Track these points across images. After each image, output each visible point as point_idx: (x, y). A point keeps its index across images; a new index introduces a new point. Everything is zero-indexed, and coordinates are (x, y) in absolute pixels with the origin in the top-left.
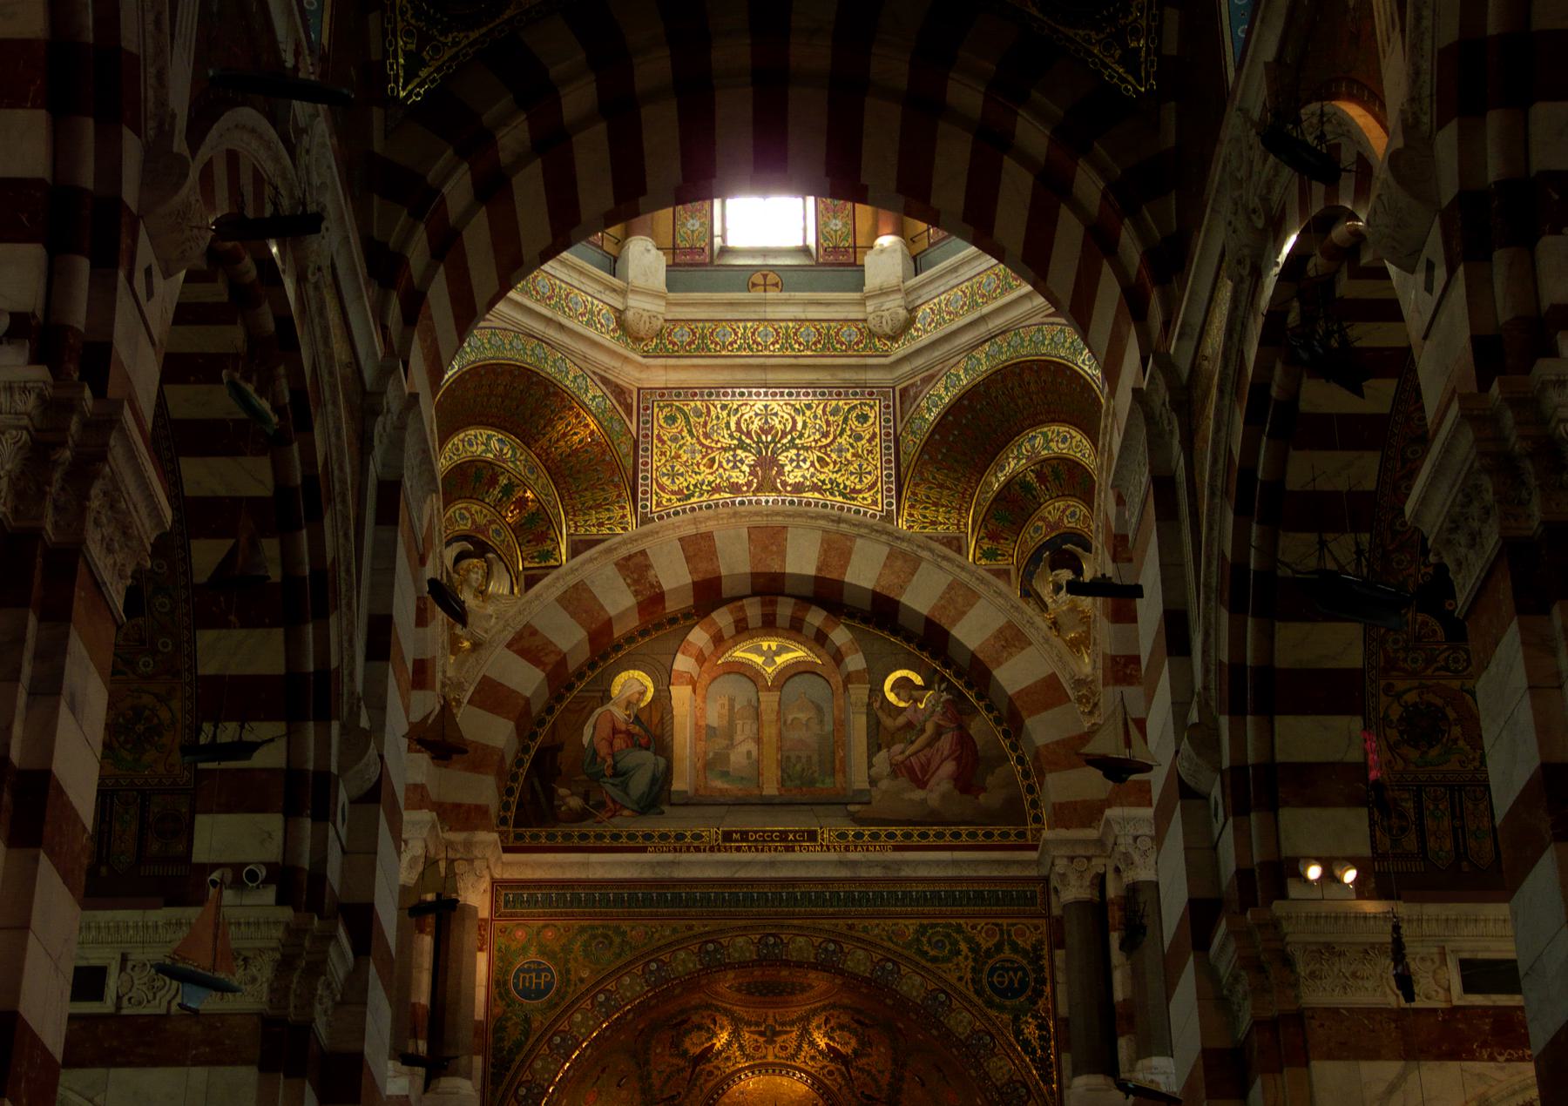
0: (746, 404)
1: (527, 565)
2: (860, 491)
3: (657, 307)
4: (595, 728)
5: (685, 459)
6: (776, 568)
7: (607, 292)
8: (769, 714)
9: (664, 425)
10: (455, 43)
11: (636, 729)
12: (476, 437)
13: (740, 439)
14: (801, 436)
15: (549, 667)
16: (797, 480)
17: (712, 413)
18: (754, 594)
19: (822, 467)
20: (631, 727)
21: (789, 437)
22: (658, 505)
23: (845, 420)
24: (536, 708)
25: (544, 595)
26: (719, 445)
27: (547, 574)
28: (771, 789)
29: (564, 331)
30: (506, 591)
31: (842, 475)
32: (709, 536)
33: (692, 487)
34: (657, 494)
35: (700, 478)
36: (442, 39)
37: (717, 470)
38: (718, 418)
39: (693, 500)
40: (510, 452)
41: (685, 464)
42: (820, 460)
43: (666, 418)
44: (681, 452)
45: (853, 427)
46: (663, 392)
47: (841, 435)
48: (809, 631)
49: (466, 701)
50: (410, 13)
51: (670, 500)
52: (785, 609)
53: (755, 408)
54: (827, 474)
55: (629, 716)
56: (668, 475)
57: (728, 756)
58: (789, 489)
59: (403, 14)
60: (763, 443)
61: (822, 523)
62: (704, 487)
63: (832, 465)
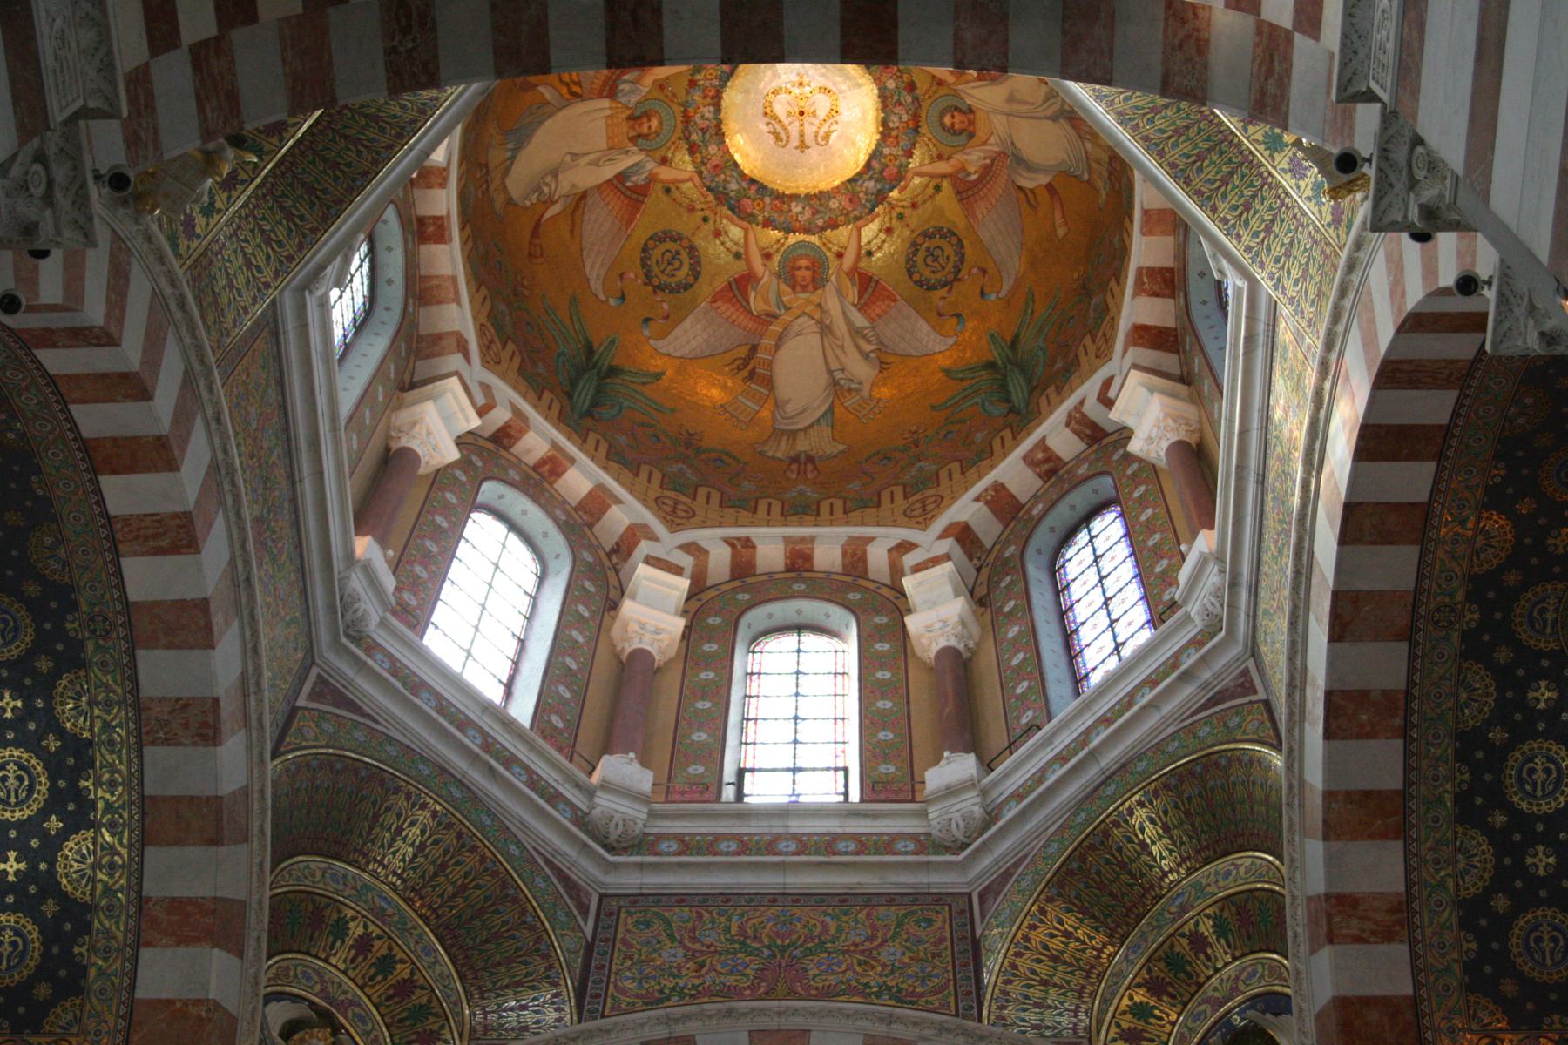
2: (922, 995)
7: (567, 785)
23: (900, 924)
26: (713, 949)
29: (494, 776)
33: (667, 991)
34: (613, 998)
35: (681, 982)
37: (707, 973)
38: (713, 923)
44: (655, 955)
46: (636, 899)
47: (893, 939)
54: (873, 978)
60: (777, 947)
61: (861, 1023)
63: (879, 969)
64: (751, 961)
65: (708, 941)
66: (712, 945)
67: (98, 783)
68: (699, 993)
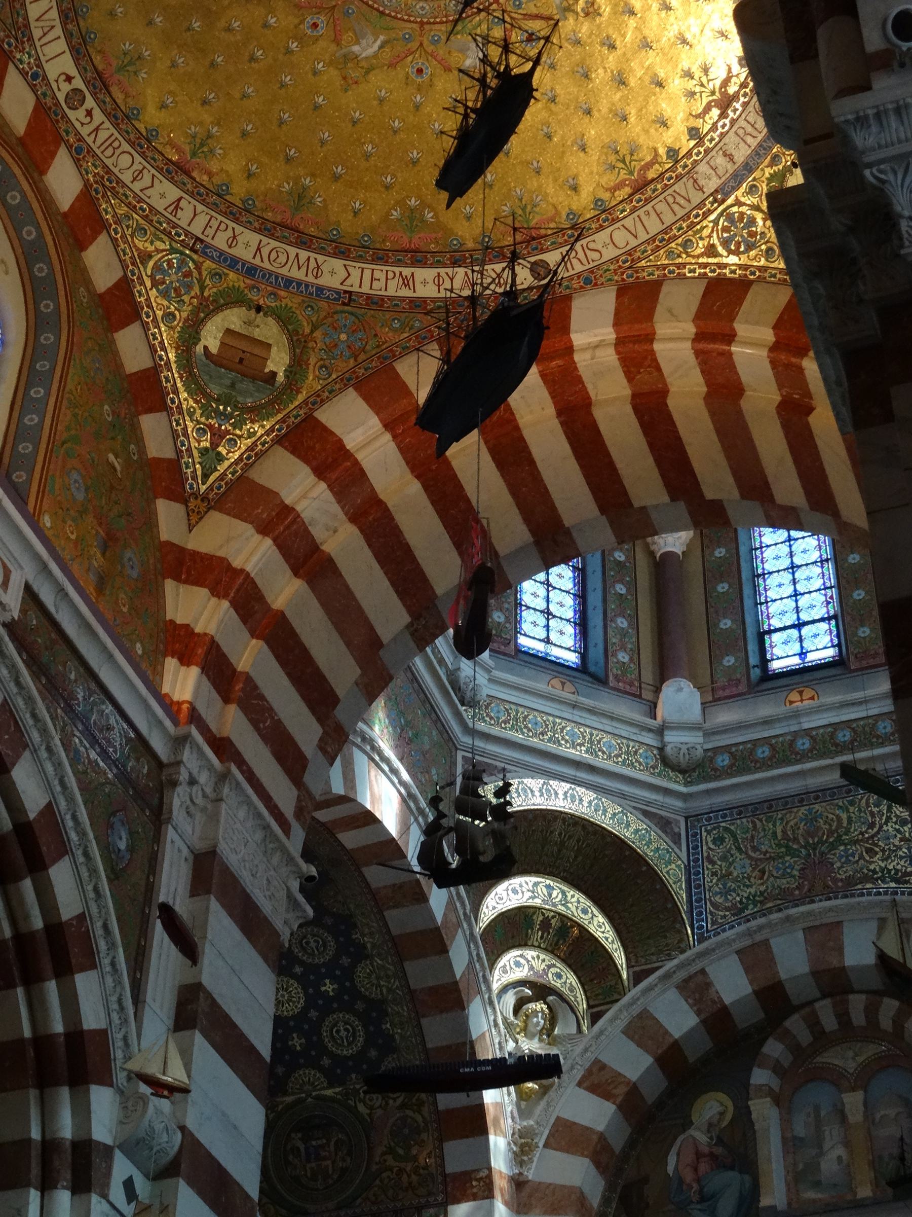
0: (791, 812)
1: (592, 1003)
3: (694, 739)
4: (678, 1155)
5: (735, 874)
6: (835, 963)
8: (855, 1115)
9: (712, 846)
10: (251, 435)
11: (719, 1150)
12: (521, 886)
13: (787, 847)
14: (847, 832)
15: (619, 1100)
16: (848, 874)
17: (758, 826)
18: (824, 996)
19: (871, 857)
20: (714, 1150)
21: (835, 835)
22: (713, 923)
24: (617, 1143)
25: (610, 1029)
26: (768, 855)
27: (607, 1010)
28: (865, 1192)
30: (574, 1030)
31: (892, 861)
32: (766, 943)
33: (744, 900)
34: (711, 913)
35: (753, 890)
36: (238, 432)
37: (768, 879)
38: (764, 830)
39: (747, 912)
40: (560, 896)
41: (735, 880)
42: (869, 851)
43: (714, 841)
45: (898, 812)
47: (886, 823)
48: (886, 1024)
49: (541, 1145)
50: (199, 412)
51: (725, 916)
52: (857, 1003)
53: (800, 814)
55: (711, 1138)
56: (720, 893)
57: (819, 1164)
58: (840, 884)
59: (191, 415)
62: (757, 898)
64: (795, 862)
65: (763, 848)
66: (767, 852)
67: (363, 935)
68: (766, 898)
